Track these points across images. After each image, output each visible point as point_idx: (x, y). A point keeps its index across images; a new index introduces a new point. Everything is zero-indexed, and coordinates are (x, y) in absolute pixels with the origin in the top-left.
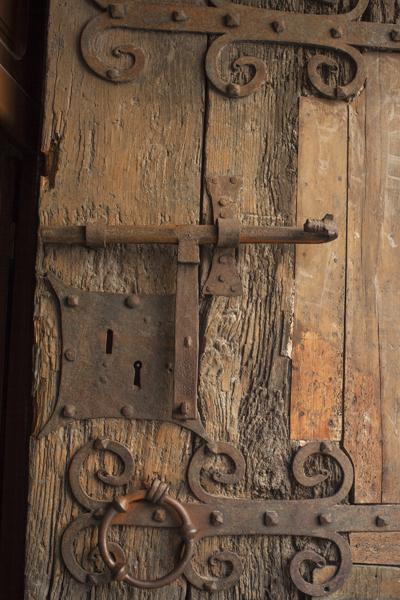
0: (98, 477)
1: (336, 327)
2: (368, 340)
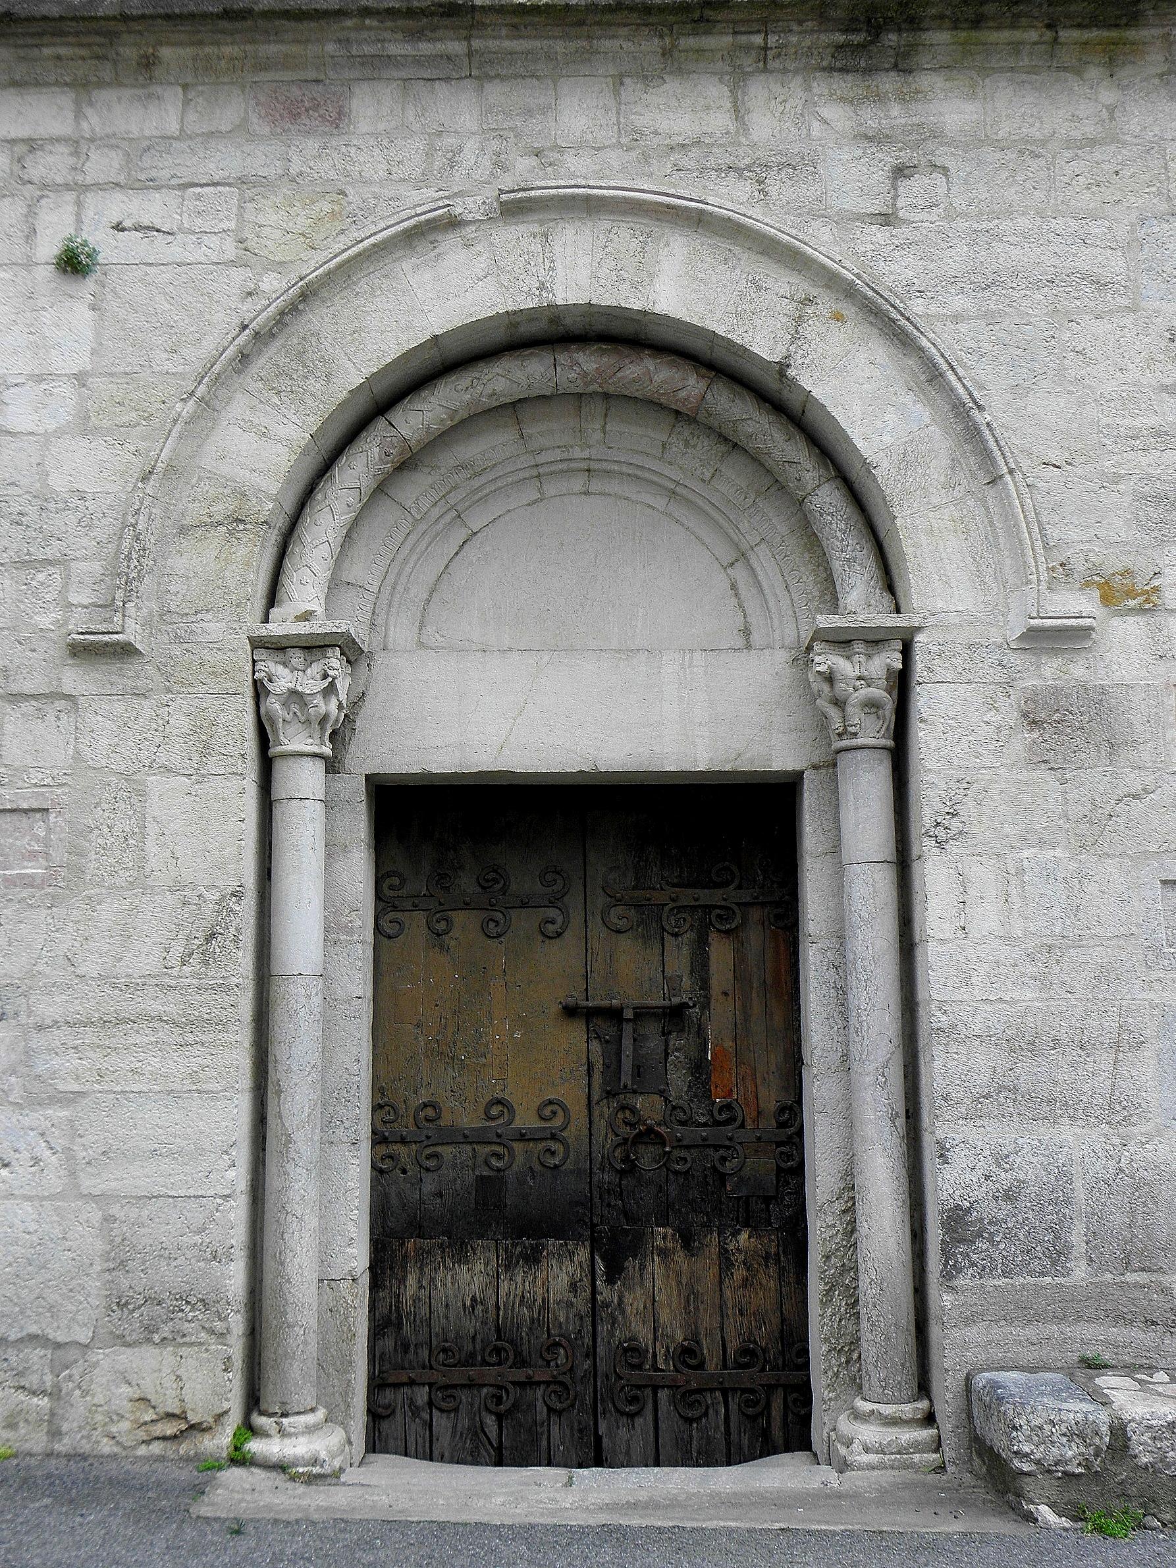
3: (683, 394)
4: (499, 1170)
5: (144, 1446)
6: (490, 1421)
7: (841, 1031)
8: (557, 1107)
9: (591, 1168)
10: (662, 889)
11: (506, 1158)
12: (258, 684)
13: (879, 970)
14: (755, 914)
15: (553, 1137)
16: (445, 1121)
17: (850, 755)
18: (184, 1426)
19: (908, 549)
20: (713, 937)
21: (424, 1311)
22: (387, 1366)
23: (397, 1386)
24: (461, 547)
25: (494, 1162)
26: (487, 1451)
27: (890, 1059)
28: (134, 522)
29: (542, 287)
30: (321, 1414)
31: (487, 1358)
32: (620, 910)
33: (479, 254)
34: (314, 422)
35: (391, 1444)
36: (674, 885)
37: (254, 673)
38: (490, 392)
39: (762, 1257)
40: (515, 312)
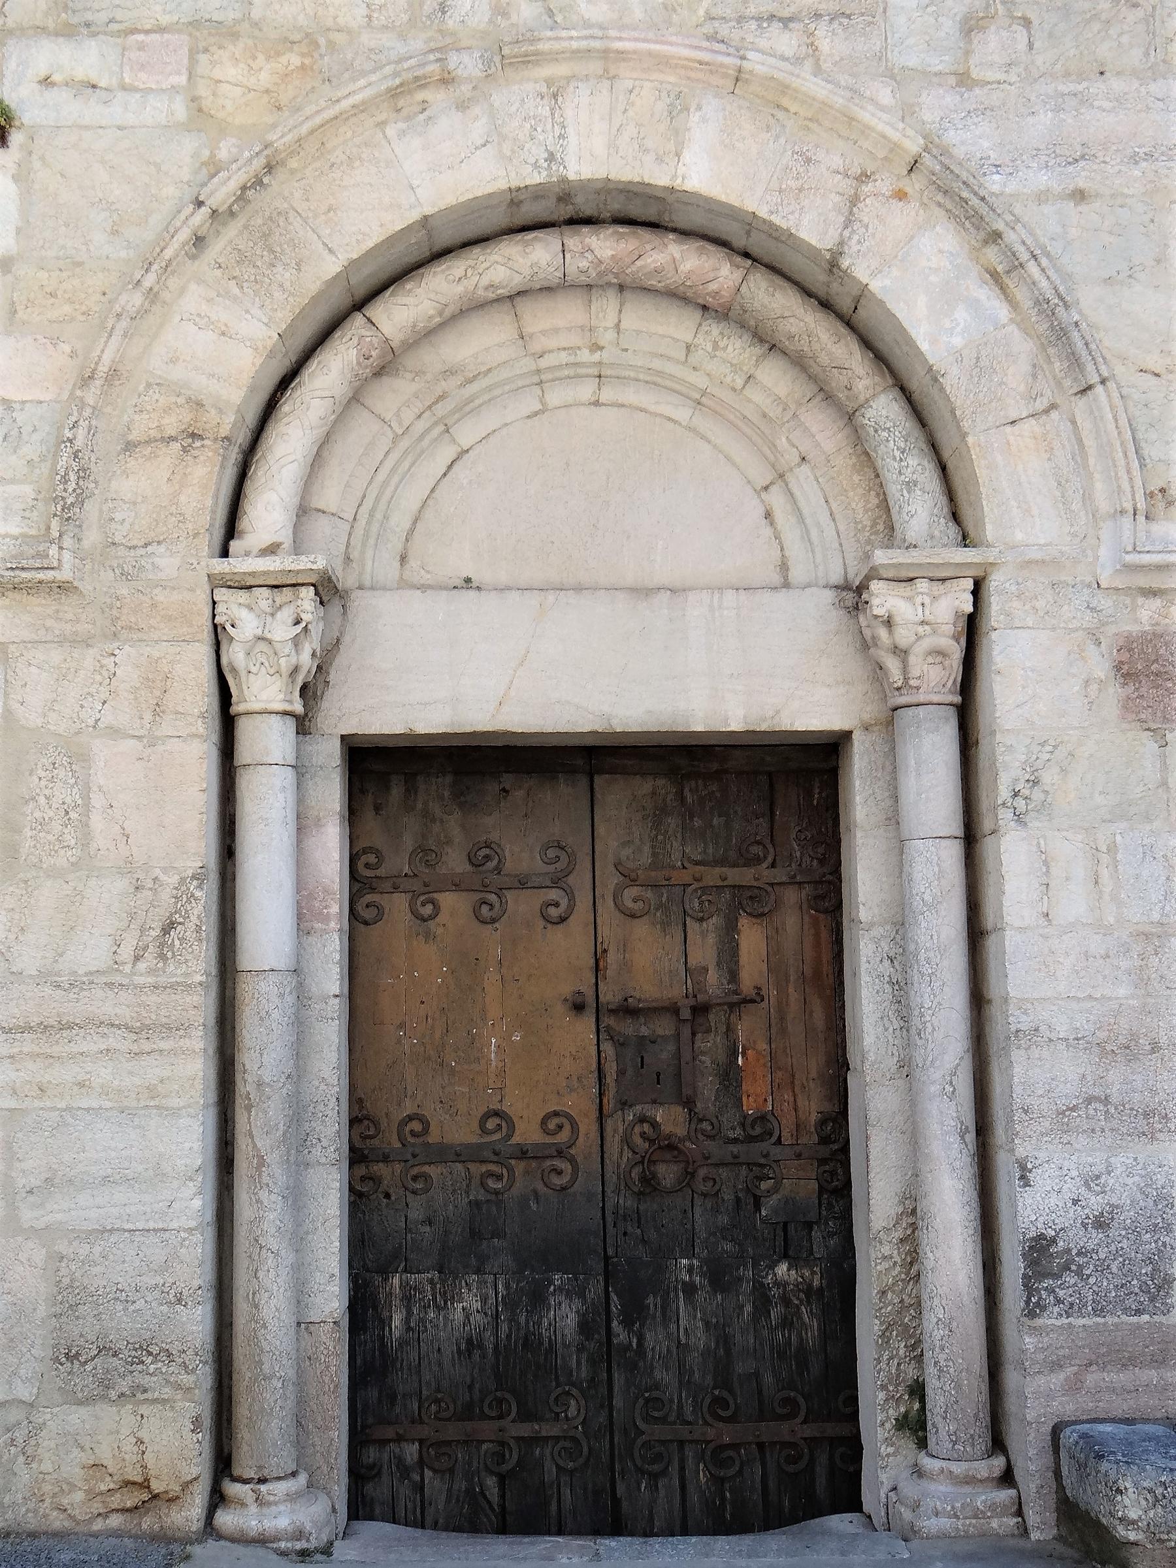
0: (643, 1135)
1: (765, 1046)
2: (785, 1051)
3: (713, 286)
4: (497, 1193)
5: (100, 1519)
6: (491, 1482)
7: (898, 1032)
8: (564, 1120)
9: (603, 1192)
10: (684, 867)
11: (505, 1180)
12: (219, 630)
13: (945, 963)
14: (791, 896)
15: (560, 1154)
16: (433, 1138)
17: (910, 712)
18: (145, 1496)
19: (982, 473)
20: (744, 922)
21: (414, 1355)
22: (370, 1421)
23: (383, 1442)
24: (450, 467)
25: (492, 1184)
26: (486, 1515)
27: (958, 1065)
28: (71, 436)
29: (551, 158)
30: (302, 1479)
31: (486, 1410)
32: (634, 891)
33: (477, 118)
34: (284, 318)
35: (377, 1511)
36: (697, 863)
37: (214, 616)
38: (487, 283)
39: (803, 1291)
40: (519, 189)
